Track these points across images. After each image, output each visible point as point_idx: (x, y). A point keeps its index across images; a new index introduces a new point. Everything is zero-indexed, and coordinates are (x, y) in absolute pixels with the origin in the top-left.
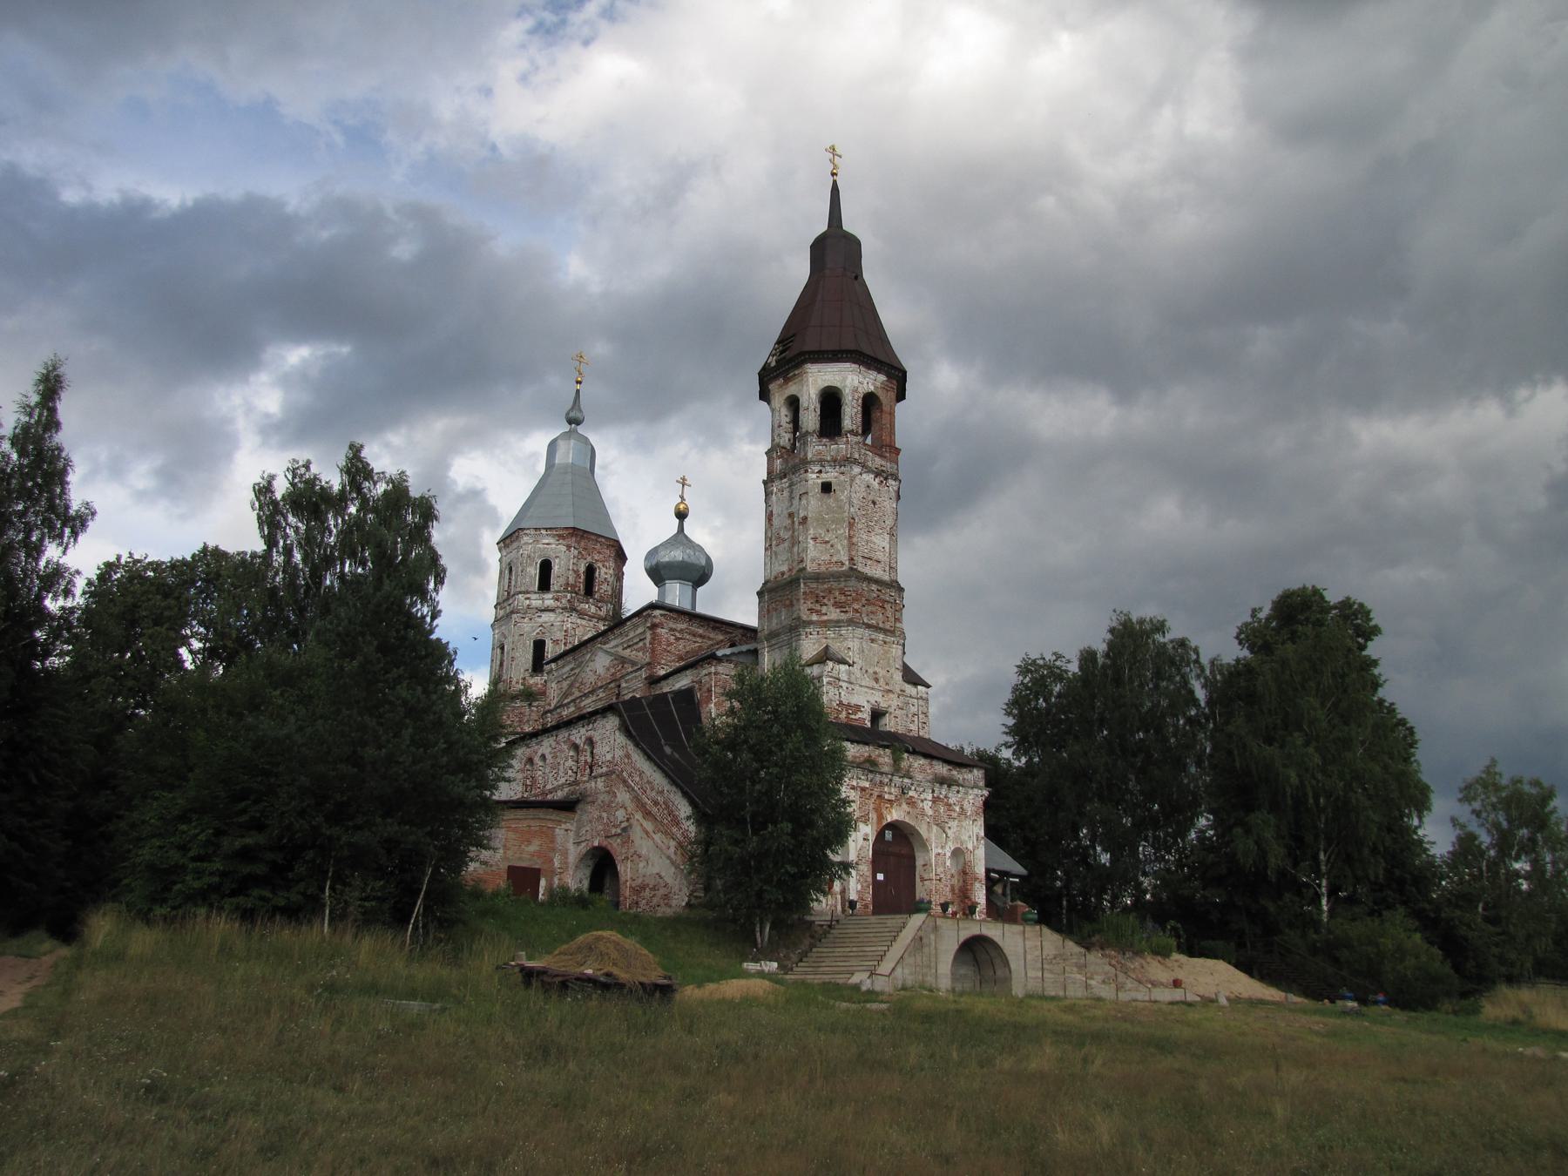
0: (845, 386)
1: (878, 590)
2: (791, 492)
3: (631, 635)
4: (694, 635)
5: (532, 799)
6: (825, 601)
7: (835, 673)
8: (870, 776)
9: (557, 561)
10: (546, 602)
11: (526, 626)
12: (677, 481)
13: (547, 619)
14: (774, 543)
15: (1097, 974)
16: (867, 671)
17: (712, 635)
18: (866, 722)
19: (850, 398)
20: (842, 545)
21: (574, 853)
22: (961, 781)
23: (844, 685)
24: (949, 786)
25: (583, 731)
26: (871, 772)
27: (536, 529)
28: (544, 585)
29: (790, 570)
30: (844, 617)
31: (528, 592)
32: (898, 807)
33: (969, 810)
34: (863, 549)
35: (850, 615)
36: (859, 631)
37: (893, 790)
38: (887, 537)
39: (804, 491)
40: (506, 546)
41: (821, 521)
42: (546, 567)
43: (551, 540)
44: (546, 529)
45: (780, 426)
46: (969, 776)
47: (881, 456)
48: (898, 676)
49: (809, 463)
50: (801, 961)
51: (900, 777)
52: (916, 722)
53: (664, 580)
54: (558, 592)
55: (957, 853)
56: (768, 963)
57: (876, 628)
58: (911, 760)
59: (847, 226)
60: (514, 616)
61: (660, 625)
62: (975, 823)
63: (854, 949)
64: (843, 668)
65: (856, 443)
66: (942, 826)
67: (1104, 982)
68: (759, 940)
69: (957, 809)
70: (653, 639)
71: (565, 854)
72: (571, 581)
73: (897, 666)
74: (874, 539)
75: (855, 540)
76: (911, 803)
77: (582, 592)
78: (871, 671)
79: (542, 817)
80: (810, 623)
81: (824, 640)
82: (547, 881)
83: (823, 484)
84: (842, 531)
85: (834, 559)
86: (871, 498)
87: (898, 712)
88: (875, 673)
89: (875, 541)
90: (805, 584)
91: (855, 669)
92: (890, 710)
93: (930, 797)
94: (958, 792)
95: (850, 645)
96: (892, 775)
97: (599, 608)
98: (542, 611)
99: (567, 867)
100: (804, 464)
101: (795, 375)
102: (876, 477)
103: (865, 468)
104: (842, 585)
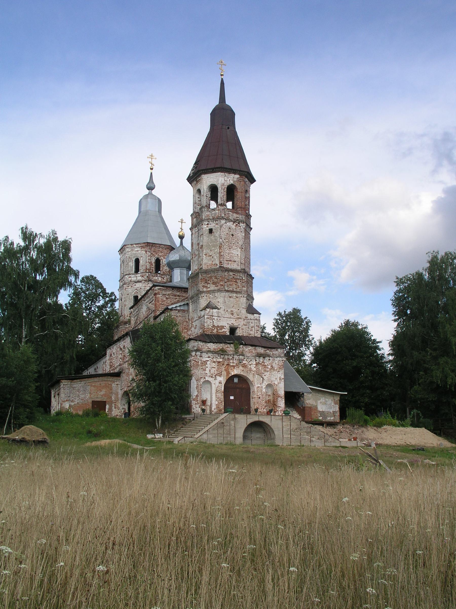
0: (218, 183)
2: (198, 234)
3: (151, 297)
4: (175, 296)
5: (111, 372)
6: (209, 282)
7: (210, 314)
8: (222, 356)
9: (142, 258)
10: (138, 278)
12: (179, 222)
13: (138, 286)
14: (194, 256)
15: (315, 435)
17: (184, 295)
18: (227, 333)
19: (220, 189)
21: (120, 393)
22: (271, 355)
23: (216, 318)
24: (264, 358)
25: (123, 342)
26: (222, 355)
27: (131, 245)
28: (137, 270)
29: (198, 268)
30: (216, 288)
31: (130, 274)
32: (237, 368)
33: (276, 367)
34: (227, 257)
35: (218, 287)
36: (223, 294)
37: (235, 361)
38: (239, 250)
40: (122, 253)
41: (208, 247)
42: (137, 261)
43: (139, 249)
45: (195, 203)
46: (275, 352)
47: (237, 213)
48: (244, 311)
49: (203, 221)
50: (174, 433)
51: (238, 356)
52: (253, 330)
53: (173, 269)
54: (143, 273)
55: (269, 386)
56: (158, 434)
57: (232, 292)
58: (244, 348)
59: (228, 102)
60: (125, 286)
63: (194, 428)
65: (224, 209)
66: (260, 375)
67: (318, 439)
69: (269, 367)
70: (155, 300)
71: (117, 394)
72: (148, 267)
73: (243, 307)
74: (232, 252)
75: (222, 254)
76: (244, 366)
77: (154, 272)
78: (229, 310)
79: (106, 380)
80: (203, 292)
81: (209, 299)
83: (209, 229)
84: (217, 250)
85: (214, 263)
86: (231, 233)
87: (244, 327)
88: (232, 311)
89: (233, 252)
90: (201, 275)
91: (221, 311)
92: (239, 326)
93: (255, 363)
94: (269, 360)
95: (219, 300)
97: (163, 278)
98: (136, 282)
99: (118, 400)
100: (202, 220)
101: (199, 180)
102: (234, 223)
103: (228, 220)
104: (216, 274)
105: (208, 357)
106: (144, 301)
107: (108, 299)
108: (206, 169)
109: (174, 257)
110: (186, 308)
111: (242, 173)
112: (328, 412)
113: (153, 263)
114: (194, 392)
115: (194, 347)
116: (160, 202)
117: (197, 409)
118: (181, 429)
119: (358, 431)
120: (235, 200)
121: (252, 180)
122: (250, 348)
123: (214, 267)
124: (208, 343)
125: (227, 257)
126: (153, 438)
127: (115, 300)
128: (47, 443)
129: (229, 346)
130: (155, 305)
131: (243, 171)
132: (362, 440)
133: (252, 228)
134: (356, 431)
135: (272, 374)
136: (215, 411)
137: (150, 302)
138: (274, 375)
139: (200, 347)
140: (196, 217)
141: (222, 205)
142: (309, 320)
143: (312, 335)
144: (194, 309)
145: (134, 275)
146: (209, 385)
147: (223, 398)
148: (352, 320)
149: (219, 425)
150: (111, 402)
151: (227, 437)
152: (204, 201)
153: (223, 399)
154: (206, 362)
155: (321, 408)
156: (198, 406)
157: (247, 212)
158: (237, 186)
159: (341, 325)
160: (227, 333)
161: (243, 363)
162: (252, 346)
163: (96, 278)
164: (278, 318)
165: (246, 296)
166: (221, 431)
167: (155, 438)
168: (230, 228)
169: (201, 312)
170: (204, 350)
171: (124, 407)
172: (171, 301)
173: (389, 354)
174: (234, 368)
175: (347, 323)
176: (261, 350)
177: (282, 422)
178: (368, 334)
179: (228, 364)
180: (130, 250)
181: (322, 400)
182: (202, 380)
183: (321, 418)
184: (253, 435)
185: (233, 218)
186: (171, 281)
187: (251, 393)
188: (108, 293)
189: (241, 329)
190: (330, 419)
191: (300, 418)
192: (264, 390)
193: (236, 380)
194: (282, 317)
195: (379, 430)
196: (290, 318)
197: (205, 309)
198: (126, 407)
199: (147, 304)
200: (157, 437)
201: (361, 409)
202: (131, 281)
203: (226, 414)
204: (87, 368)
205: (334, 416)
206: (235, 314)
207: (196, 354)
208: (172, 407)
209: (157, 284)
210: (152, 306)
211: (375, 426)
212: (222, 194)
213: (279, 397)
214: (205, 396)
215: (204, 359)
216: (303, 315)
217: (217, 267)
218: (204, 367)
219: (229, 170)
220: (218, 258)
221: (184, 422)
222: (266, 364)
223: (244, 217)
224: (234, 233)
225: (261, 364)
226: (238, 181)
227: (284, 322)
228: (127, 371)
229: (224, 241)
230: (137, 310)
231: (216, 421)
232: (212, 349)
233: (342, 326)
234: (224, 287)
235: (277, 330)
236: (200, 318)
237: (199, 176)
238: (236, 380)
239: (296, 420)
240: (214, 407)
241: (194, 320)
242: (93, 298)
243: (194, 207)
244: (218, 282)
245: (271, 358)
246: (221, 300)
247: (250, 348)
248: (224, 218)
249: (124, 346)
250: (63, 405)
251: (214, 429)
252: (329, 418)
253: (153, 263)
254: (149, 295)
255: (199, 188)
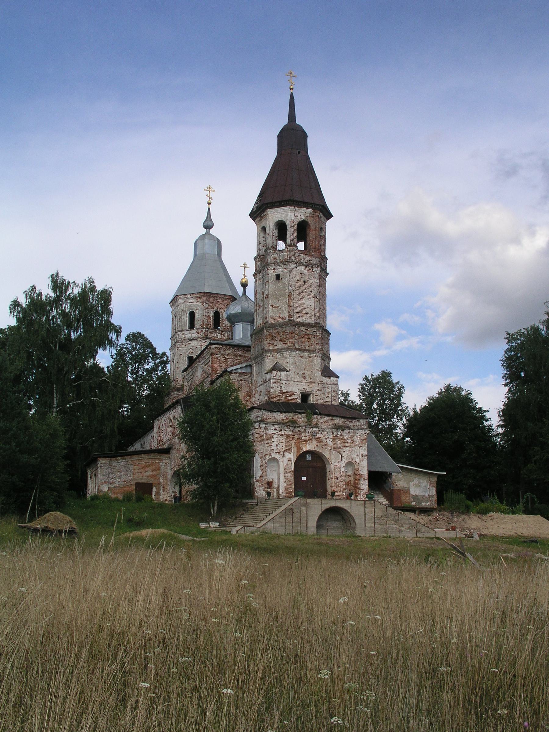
0: (287, 220)
1: (305, 329)
2: (263, 280)
3: (207, 358)
4: (236, 356)
5: (160, 448)
6: (276, 339)
7: (277, 377)
8: (291, 429)
9: (197, 311)
10: (193, 335)
11: (183, 349)
12: (241, 266)
13: (193, 345)
14: (258, 308)
16: (298, 374)
18: (298, 400)
19: (290, 226)
20: (285, 308)
21: (170, 473)
22: (352, 427)
23: (284, 382)
24: (343, 430)
27: (185, 295)
28: (192, 326)
29: (263, 322)
30: (284, 346)
31: (183, 331)
32: (310, 443)
33: (357, 441)
34: (297, 308)
35: (287, 345)
36: (293, 353)
37: (307, 434)
38: (313, 300)
39: (267, 280)
40: (173, 305)
42: (192, 315)
43: (194, 300)
44: (190, 294)
45: (260, 244)
46: (357, 423)
47: (310, 255)
48: (318, 374)
49: (269, 265)
50: (233, 522)
51: (311, 428)
52: (330, 397)
53: (235, 323)
55: (349, 464)
56: (213, 523)
57: (304, 350)
58: (319, 418)
59: (299, 121)
60: (177, 344)
61: (216, 353)
62: (361, 448)
63: (257, 515)
64: (283, 373)
65: (294, 251)
66: (338, 450)
68: (213, 513)
69: (349, 441)
70: (212, 361)
71: (166, 475)
72: (205, 322)
75: (292, 304)
76: (319, 440)
78: (301, 373)
79: (152, 457)
80: (269, 351)
81: (276, 359)
82: (156, 488)
83: (276, 275)
84: (285, 300)
85: (281, 316)
86: (302, 279)
87: (318, 393)
88: (304, 374)
89: (305, 302)
90: (266, 330)
92: (313, 392)
93: (331, 436)
94: (349, 432)
95: (288, 360)
96: (306, 427)
97: (223, 335)
98: (190, 340)
100: (267, 264)
101: (264, 215)
102: (306, 267)
103: (299, 263)
104: (284, 329)
105: (275, 430)
106: (200, 362)
107: (158, 361)
108: (272, 203)
109: (235, 309)
110: (248, 370)
111: (316, 206)
112: (423, 497)
113: (211, 316)
114: (257, 472)
115: (257, 417)
116: (219, 243)
117: (261, 492)
118: (242, 516)
119: (458, 519)
120: (308, 239)
121: (328, 215)
122: (325, 419)
123: (282, 321)
124: (275, 413)
125: (297, 308)
126: (207, 528)
127: (166, 362)
128: (75, 533)
129: (300, 416)
130: (212, 367)
131: (317, 205)
132: (462, 530)
133: (328, 274)
134: (455, 519)
135: (353, 450)
136: (284, 494)
137: (207, 364)
138: (355, 451)
139: (265, 417)
140: (260, 261)
141: (291, 245)
142: (402, 385)
143: (405, 404)
144: (258, 371)
145: (188, 332)
146: (275, 464)
147: (293, 479)
148: (454, 385)
149: (287, 512)
150: (160, 484)
151: (297, 526)
152: (270, 241)
153: (292, 480)
154: (272, 436)
155: (414, 491)
156: (262, 488)
157: (322, 254)
158: (309, 222)
159: (440, 391)
160: (298, 400)
161: (317, 437)
162: (328, 415)
163: (144, 335)
164: (364, 382)
165: (321, 355)
166: (289, 519)
167: (210, 527)
168: (301, 274)
169: (266, 375)
170: (269, 421)
171: (174, 490)
172: (231, 362)
173: (498, 426)
174: (306, 443)
175: (448, 388)
176: (339, 421)
177: (365, 508)
178: (471, 401)
179: (299, 438)
180: (183, 302)
181: (416, 481)
182: (268, 457)
183: (414, 503)
184: (329, 524)
185: (304, 261)
186: (232, 339)
187: (328, 473)
188: (159, 354)
189: (314, 395)
190: (426, 504)
191: (387, 503)
192: (343, 470)
193: (309, 457)
194: (369, 381)
195: (484, 517)
196: (379, 383)
197: (271, 371)
198: (177, 490)
199: (202, 366)
200: (212, 526)
201: (462, 492)
202: (184, 338)
203: (296, 498)
204: (132, 444)
205: (430, 501)
206: (308, 378)
207: (260, 426)
208: (230, 490)
209: (215, 342)
210: (208, 369)
211: (478, 513)
212: (291, 232)
213: (361, 477)
214: (272, 476)
215: (270, 432)
216: (395, 379)
217: (286, 321)
218: (270, 441)
219: (300, 204)
220: (287, 310)
221: (245, 508)
222: (346, 438)
223: (318, 259)
224: (306, 280)
225: (339, 438)
226: (311, 216)
227: (372, 387)
228: (177, 446)
229: (295, 289)
230: (191, 374)
231: (284, 507)
232: (279, 420)
233: (442, 392)
234: (294, 345)
235: (363, 398)
236: (265, 382)
237: (264, 210)
238: (309, 457)
239: (382, 506)
240: (282, 490)
241: (258, 385)
242: (141, 359)
243: (258, 249)
244: (287, 338)
245: (351, 430)
246: (290, 360)
247: (325, 419)
248: (294, 262)
249: (174, 417)
250: (101, 488)
251: (280, 517)
252: (423, 504)
253: (211, 316)
254: (205, 355)
255: (264, 225)
